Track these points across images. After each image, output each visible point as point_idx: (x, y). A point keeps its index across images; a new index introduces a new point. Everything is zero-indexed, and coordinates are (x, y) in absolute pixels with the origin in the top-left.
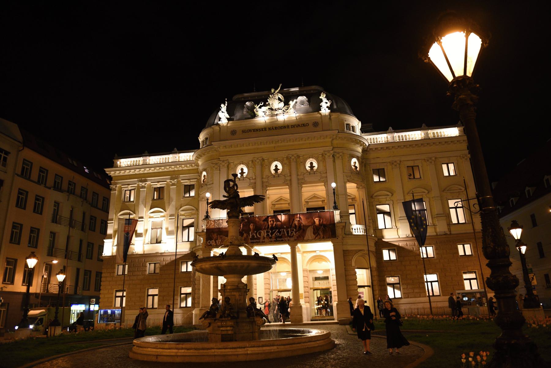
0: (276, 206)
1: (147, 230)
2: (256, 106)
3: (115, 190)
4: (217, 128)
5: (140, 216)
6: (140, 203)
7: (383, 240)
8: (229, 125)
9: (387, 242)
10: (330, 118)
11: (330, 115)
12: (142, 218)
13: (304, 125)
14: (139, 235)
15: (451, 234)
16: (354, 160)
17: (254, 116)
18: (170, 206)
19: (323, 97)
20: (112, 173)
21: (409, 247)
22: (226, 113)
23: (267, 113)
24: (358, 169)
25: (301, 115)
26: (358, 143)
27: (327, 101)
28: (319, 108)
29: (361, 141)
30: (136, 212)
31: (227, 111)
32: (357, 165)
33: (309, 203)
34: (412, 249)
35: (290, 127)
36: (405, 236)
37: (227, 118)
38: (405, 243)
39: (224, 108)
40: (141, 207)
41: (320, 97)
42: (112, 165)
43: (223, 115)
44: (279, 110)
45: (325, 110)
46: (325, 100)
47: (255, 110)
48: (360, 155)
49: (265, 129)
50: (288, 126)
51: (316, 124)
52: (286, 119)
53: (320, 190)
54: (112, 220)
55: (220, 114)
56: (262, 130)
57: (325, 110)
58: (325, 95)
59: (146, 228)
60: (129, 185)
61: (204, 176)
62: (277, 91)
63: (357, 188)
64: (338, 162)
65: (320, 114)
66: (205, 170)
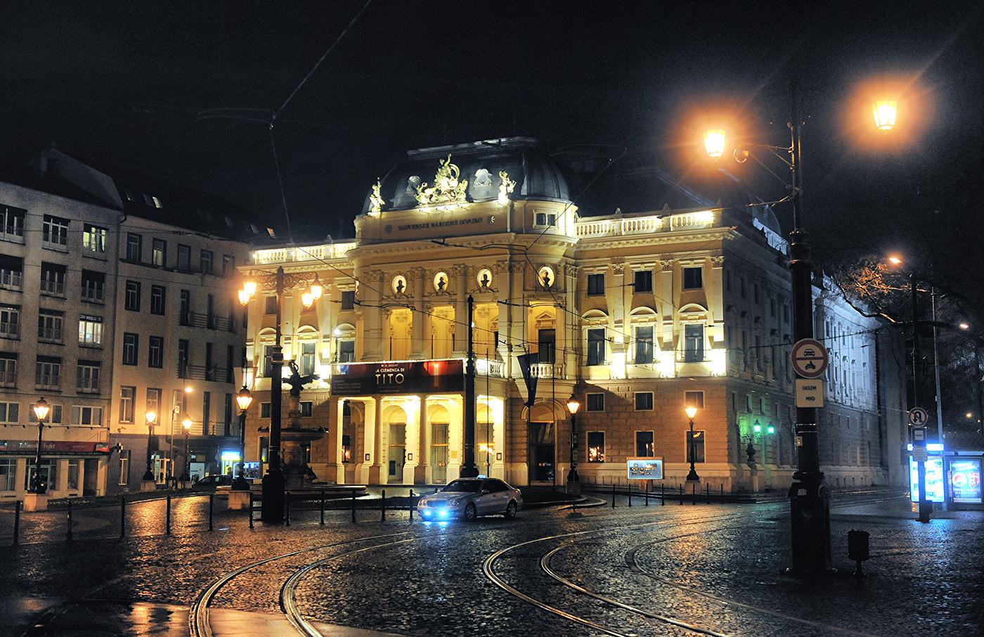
13: (476, 219)
39: (377, 190)
44: (445, 197)
49: (428, 225)
50: (456, 221)
54: (251, 340)
56: (424, 227)
64: (518, 276)
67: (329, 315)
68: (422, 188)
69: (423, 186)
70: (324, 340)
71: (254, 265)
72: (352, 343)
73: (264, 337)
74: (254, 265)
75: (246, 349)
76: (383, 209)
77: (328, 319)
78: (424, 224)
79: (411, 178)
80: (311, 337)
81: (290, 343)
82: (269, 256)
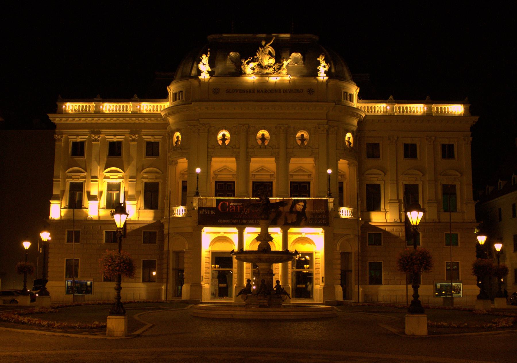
0: (257, 177)
1: (101, 193)
2: (243, 61)
3: (61, 141)
4: (195, 82)
5: (93, 175)
6: (93, 159)
7: (370, 223)
8: (210, 81)
9: (374, 226)
10: (327, 84)
11: (327, 81)
12: (96, 177)
13: (298, 91)
14: (91, 198)
15: (439, 222)
16: (349, 135)
17: (240, 73)
18: (131, 167)
19: (321, 59)
20: (57, 119)
21: (395, 233)
22: (207, 65)
23: (256, 71)
24: (352, 145)
25: (296, 78)
26: (354, 116)
27: (326, 65)
28: (315, 73)
29: (358, 114)
30: (89, 170)
31: (209, 63)
32: (351, 140)
33: (294, 177)
34: (398, 235)
35: (282, 91)
36: (392, 221)
37: (209, 72)
38: (392, 228)
39: (205, 59)
40: (94, 164)
41: (318, 59)
42: (56, 109)
43: (204, 66)
44: (270, 70)
45: (322, 76)
46: (323, 63)
47: (242, 67)
48: (355, 129)
49: (253, 91)
50: (280, 90)
51: (311, 91)
52: (278, 82)
53: (307, 163)
55: (201, 66)
57: (322, 76)
58: (324, 58)
59: (100, 190)
60: (78, 136)
61: (178, 137)
62: (269, 44)
63: (349, 164)
65: (317, 80)
66: (178, 130)
67: (135, 160)
68: (247, 61)
69: (249, 60)
70: (130, 180)
71: (62, 113)
72: (157, 184)
73: (70, 175)
74: (62, 113)
75: (53, 183)
76: (211, 73)
77: (134, 163)
78: (250, 90)
79: (231, 53)
80: (117, 177)
81: (97, 181)
82: (77, 108)
